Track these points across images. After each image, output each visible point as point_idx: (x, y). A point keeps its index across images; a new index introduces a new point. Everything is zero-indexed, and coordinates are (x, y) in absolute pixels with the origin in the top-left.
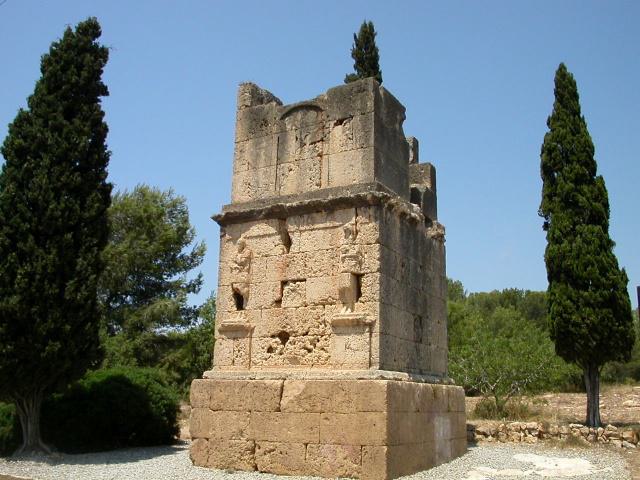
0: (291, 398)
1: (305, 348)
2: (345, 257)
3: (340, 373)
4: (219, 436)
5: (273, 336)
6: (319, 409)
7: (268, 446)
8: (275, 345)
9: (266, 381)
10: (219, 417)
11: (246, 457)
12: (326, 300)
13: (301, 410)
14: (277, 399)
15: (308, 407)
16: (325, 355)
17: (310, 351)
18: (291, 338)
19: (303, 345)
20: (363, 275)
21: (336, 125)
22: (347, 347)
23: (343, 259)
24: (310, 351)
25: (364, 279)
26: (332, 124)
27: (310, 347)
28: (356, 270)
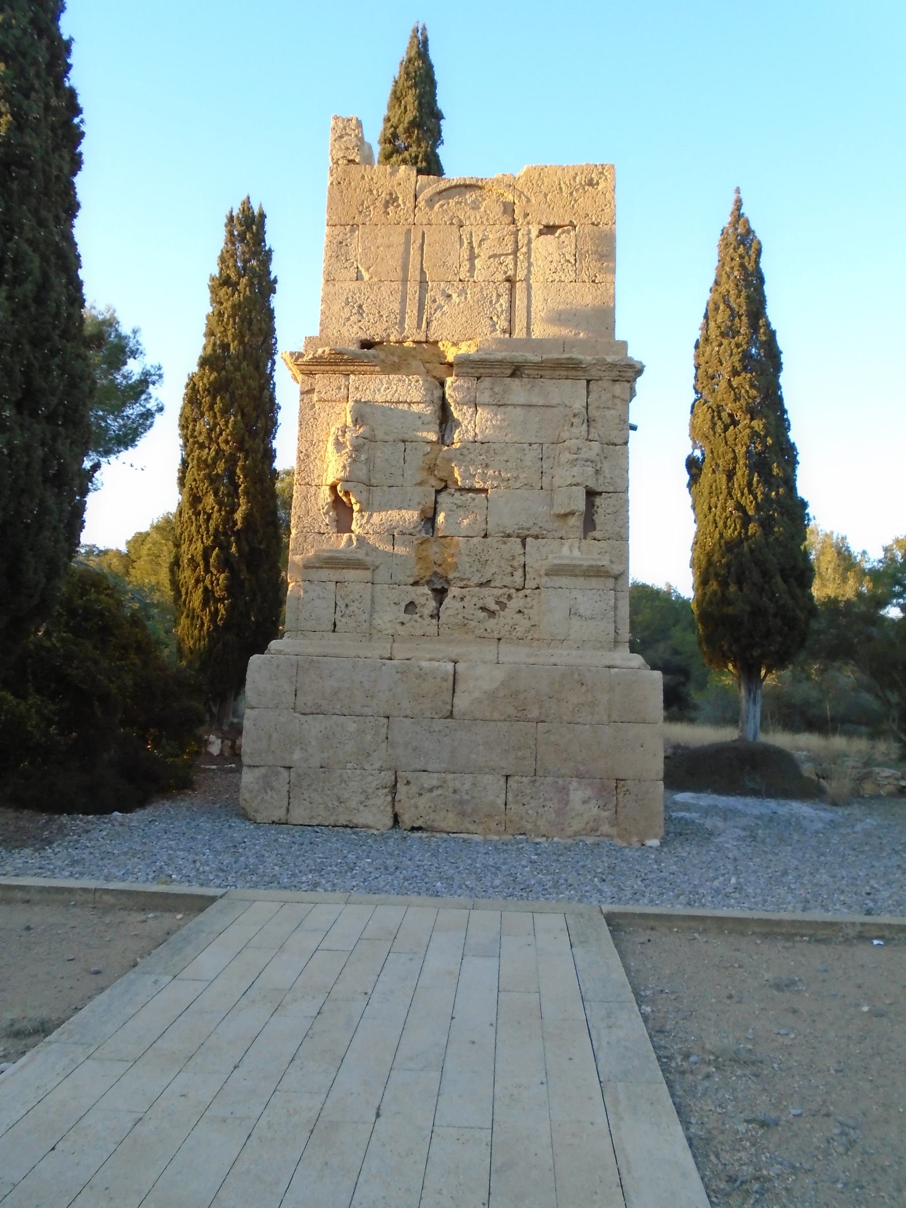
0: (477, 694)
1: (483, 609)
2: (577, 459)
3: (563, 656)
4: (315, 762)
5: (416, 584)
6: (535, 713)
7: (429, 780)
8: (422, 600)
9: (424, 664)
10: (314, 727)
11: (379, 802)
12: (528, 529)
13: (496, 715)
14: (447, 696)
15: (512, 712)
16: (524, 623)
17: (492, 614)
18: (454, 591)
19: (479, 605)
20: (600, 494)
21: (541, 233)
22: (573, 613)
23: (573, 463)
24: (492, 614)
25: (598, 501)
26: (534, 232)
27: (494, 607)
28: (591, 484)
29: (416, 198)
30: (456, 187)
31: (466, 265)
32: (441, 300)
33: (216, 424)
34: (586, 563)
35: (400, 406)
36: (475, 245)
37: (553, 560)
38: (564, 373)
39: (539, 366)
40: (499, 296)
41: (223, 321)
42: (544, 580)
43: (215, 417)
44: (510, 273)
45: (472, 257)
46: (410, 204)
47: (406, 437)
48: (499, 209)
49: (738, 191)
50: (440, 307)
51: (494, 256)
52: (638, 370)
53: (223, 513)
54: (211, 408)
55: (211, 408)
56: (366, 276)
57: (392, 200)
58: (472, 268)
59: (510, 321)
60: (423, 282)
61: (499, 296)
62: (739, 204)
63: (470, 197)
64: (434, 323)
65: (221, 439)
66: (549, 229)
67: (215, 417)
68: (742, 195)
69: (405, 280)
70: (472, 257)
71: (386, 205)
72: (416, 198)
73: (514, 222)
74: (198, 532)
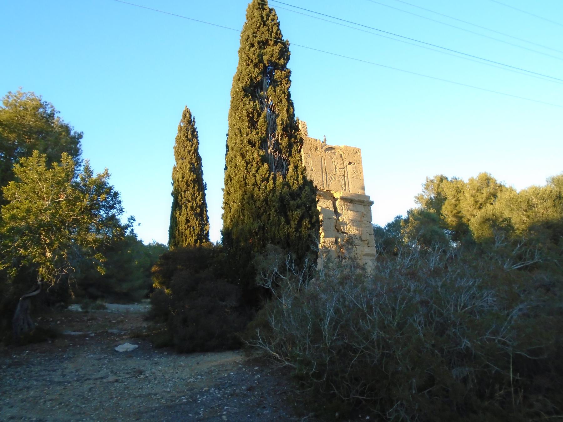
26: (347, 164)
29: (322, 149)
30: (330, 147)
31: (334, 171)
32: (330, 179)
33: (194, 194)
34: (371, 253)
35: (328, 208)
36: (336, 165)
37: (364, 253)
38: (360, 203)
39: (356, 201)
40: (342, 180)
41: (190, 154)
42: (363, 257)
43: (194, 191)
44: (344, 174)
45: (336, 168)
46: (321, 151)
47: (330, 217)
48: (340, 156)
49: (325, 136)
50: (331, 181)
51: (340, 169)
52: (372, 203)
53: (200, 227)
54: (194, 188)
55: (194, 188)
56: (314, 170)
57: (317, 149)
58: (336, 172)
59: (345, 186)
60: (326, 173)
61: (342, 180)
62: (325, 140)
63: (333, 151)
64: (330, 186)
65: (197, 200)
66: (350, 163)
67: (194, 191)
68: (326, 138)
69: (322, 172)
70: (336, 168)
71: (316, 150)
72: (322, 149)
73: (343, 160)
74: (190, 234)
